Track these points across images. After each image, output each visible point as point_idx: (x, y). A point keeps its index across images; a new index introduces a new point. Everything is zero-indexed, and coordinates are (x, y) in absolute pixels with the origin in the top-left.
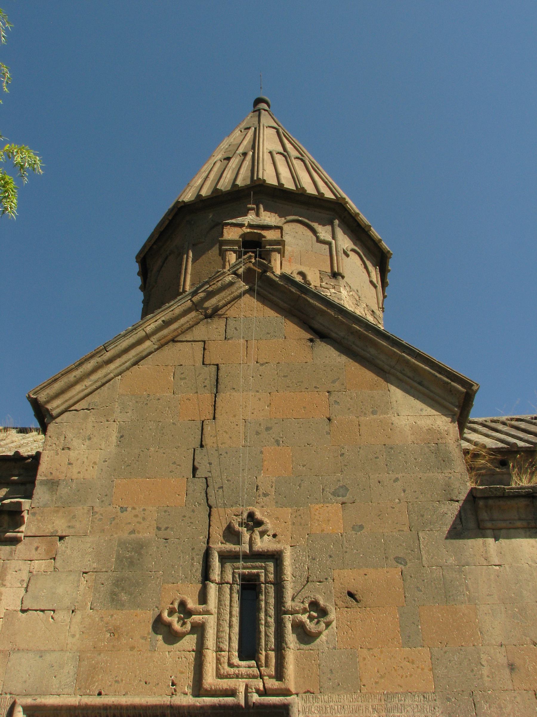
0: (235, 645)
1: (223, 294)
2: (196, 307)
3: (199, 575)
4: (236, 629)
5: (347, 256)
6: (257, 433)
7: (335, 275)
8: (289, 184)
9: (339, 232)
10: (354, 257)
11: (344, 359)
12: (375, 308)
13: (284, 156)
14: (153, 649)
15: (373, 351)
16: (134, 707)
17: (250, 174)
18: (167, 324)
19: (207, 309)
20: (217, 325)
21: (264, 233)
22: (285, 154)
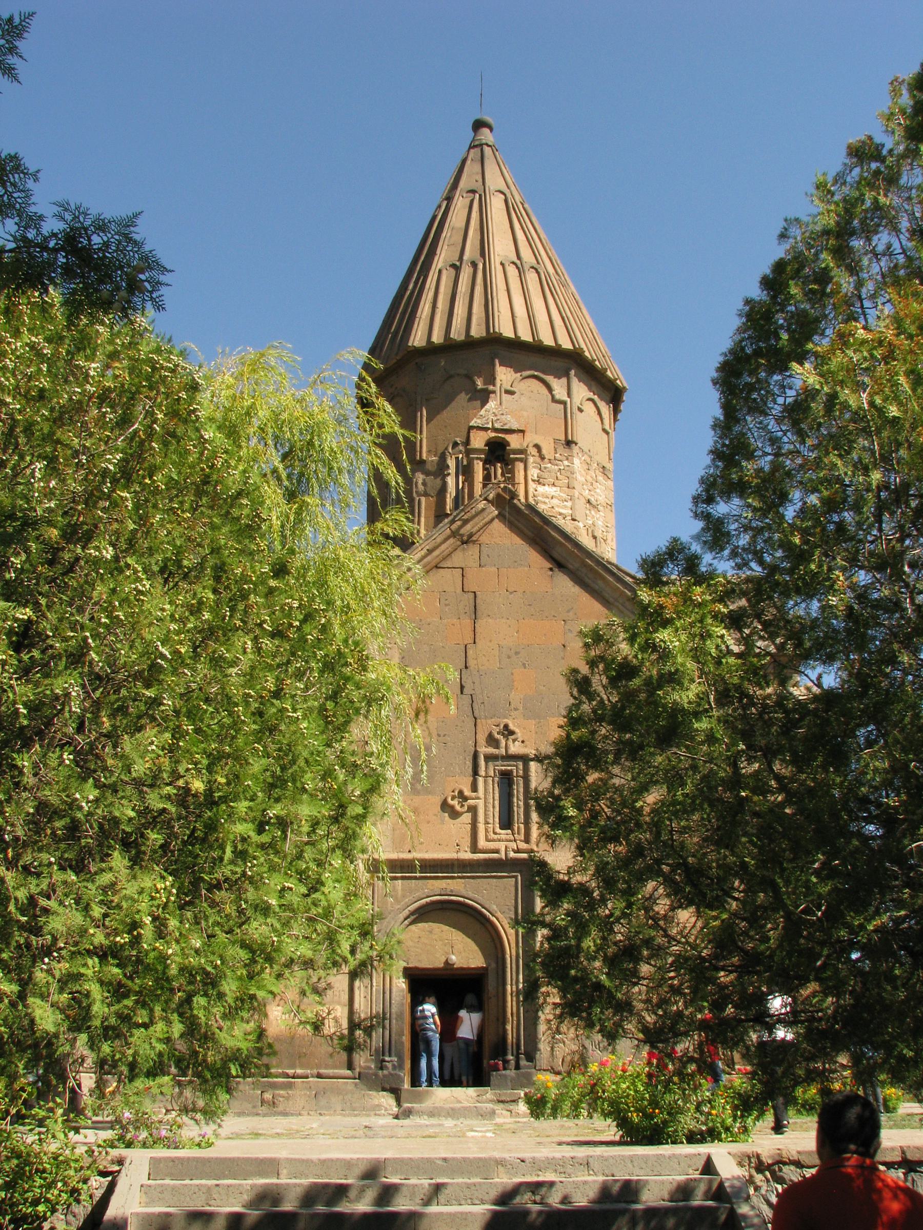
0: (497, 820)
1: (476, 519)
2: (454, 534)
3: (470, 770)
4: (497, 809)
5: (580, 410)
6: (509, 657)
7: (569, 443)
8: (526, 336)
9: (575, 382)
10: (589, 408)
11: (576, 590)
12: (604, 460)
13: (518, 268)
14: (443, 822)
15: (600, 582)
16: (434, 860)
17: (483, 314)
18: (430, 552)
19: (462, 535)
20: (473, 550)
21: (508, 437)
22: (518, 262)
